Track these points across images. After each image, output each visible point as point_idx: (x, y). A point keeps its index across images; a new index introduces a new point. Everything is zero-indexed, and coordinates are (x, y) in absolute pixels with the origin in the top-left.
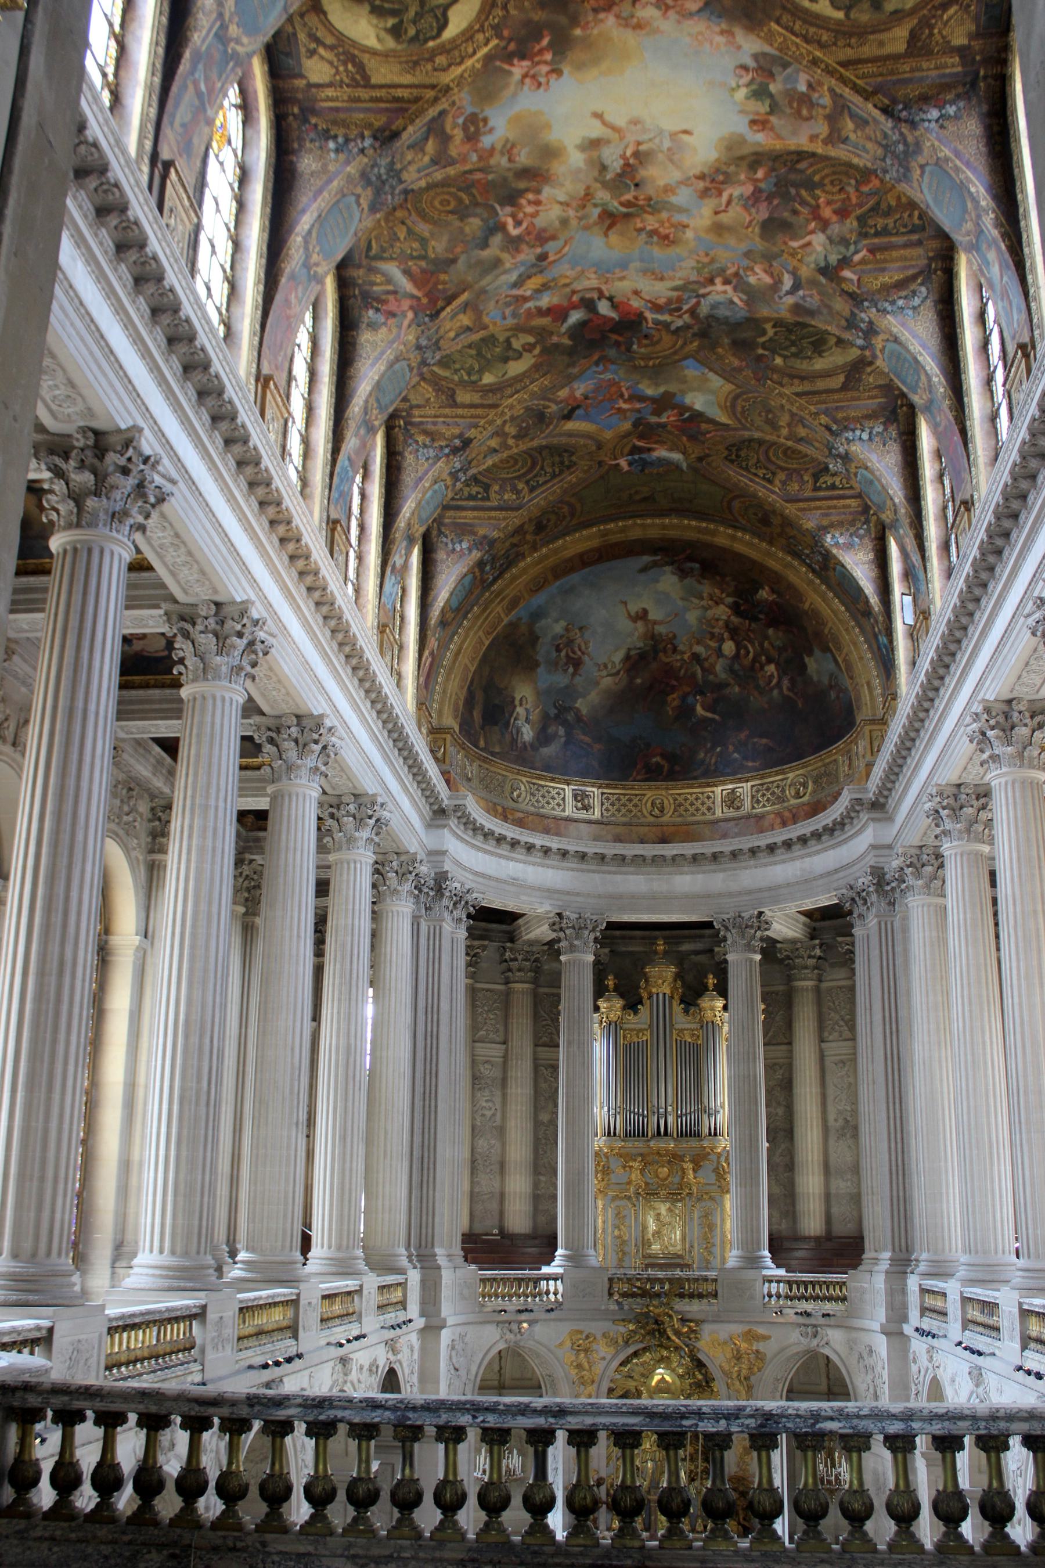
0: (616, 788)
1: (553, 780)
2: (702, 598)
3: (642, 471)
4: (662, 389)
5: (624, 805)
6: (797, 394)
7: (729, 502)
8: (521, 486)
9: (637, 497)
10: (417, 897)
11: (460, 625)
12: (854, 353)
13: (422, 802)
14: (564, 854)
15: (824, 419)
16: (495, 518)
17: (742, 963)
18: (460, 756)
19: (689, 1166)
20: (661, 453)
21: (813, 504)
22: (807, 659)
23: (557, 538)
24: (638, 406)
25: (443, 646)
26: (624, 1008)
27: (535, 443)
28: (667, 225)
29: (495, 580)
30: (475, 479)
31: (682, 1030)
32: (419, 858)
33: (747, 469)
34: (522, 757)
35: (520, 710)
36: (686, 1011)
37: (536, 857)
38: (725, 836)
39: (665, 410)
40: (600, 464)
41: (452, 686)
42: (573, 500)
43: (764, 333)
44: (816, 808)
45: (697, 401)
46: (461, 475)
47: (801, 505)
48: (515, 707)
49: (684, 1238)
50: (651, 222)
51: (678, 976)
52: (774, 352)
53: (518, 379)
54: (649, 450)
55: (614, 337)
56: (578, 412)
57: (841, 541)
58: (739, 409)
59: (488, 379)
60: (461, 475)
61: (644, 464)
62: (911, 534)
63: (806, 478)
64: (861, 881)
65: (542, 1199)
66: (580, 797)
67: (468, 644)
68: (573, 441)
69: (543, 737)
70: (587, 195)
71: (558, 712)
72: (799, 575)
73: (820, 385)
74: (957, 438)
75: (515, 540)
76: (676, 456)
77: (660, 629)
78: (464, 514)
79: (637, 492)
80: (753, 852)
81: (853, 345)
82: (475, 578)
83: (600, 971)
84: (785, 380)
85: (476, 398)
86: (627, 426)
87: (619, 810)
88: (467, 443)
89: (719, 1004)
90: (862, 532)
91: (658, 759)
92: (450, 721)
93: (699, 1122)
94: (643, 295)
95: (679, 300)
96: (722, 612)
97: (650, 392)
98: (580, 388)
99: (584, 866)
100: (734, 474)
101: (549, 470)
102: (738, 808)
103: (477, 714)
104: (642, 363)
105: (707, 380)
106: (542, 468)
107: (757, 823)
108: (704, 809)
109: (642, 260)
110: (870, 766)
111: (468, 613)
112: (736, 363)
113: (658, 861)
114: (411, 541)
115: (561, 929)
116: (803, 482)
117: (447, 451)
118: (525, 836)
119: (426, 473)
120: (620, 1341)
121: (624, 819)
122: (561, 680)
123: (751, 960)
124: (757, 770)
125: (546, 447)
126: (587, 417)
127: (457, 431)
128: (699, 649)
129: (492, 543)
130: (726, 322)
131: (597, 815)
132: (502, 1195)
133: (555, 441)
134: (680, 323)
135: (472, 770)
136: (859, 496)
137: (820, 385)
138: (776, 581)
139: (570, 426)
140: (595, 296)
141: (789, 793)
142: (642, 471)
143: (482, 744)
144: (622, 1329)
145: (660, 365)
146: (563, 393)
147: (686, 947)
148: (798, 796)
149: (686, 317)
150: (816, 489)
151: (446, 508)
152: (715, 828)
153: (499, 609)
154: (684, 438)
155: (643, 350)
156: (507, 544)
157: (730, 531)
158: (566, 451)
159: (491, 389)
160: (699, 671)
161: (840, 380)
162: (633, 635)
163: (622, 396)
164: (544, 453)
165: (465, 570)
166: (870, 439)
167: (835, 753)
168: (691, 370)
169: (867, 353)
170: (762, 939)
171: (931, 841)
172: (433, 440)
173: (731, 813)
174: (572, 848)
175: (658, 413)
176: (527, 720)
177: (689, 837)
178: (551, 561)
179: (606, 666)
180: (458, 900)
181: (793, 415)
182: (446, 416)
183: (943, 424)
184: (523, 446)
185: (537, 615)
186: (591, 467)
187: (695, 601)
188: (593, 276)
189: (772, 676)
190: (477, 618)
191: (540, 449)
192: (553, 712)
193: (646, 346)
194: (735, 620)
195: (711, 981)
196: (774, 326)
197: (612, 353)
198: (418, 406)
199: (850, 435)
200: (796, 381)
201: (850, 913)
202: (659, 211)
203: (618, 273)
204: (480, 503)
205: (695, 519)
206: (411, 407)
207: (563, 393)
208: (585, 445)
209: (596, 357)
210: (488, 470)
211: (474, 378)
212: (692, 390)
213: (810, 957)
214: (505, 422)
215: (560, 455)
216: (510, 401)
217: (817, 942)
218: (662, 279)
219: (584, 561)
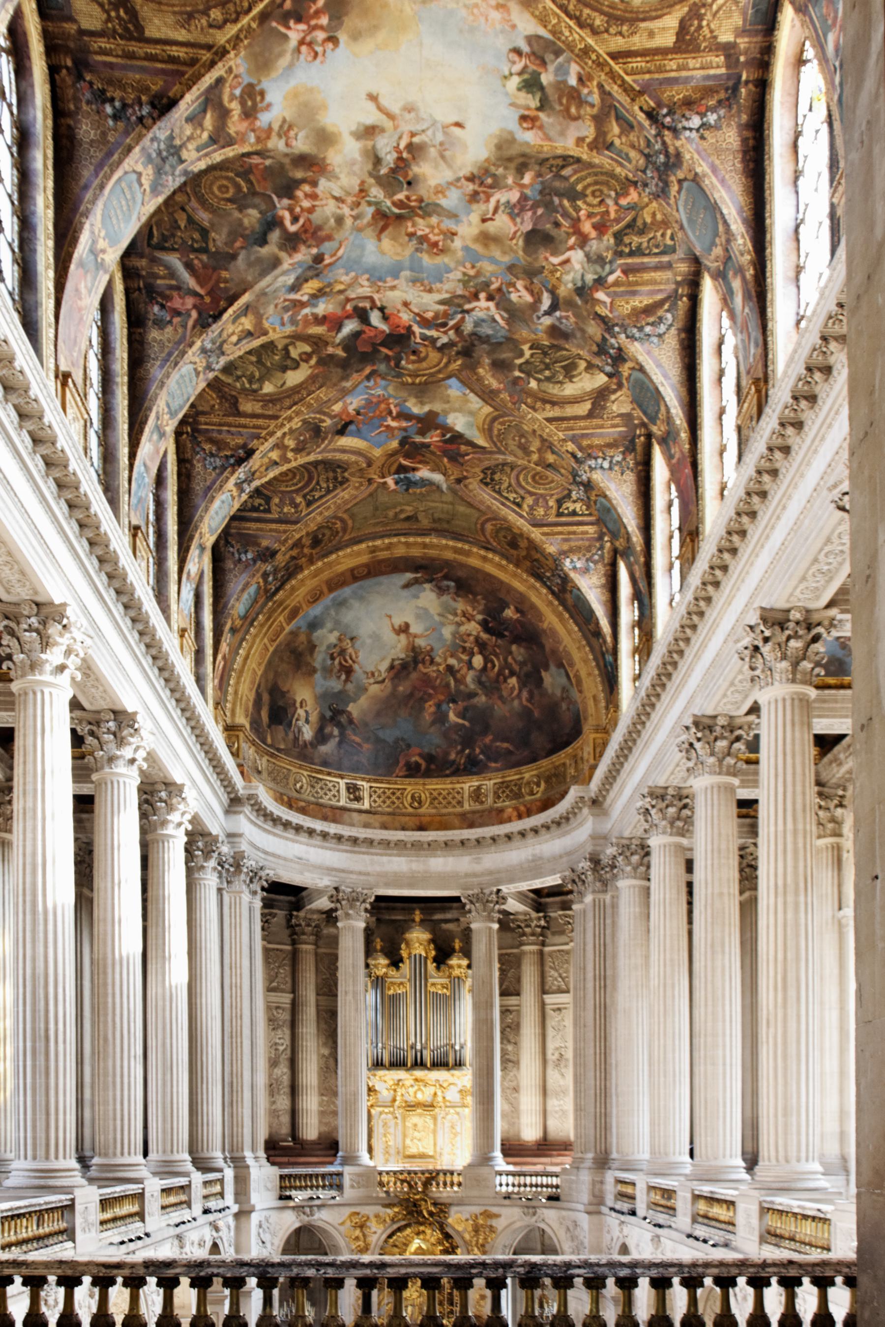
2: (456, 615)
3: (407, 490)
4: (426, 408)
7: (483, 524)
8: (299, 500)
16: (275, 531)
20: (424, 473)
23: (331, 553)
24: (404, 424)
28: (436, 231)
30: (257, 492)
33: (499, 492)
39: (429, 430)
40: (370, 481)
42: (345, 516)
45: (458, 422)
46: (245, 486)
50: (421, 226)
54: (414, 469)
56: (352, 428)
59: (268, 388)
61: (409, 484)
70: (361, 191)
76: (438, 477)
78: (248, 525)
79: (402, 511)
86: (395, 444)
94: (412, 307)
95: (446, 315)
97: (416, 410)
105: (467, 401)
106: (318, 483)
109: (412, 269)
113: (417, 846)
125: (324, 462)
130: (485, 340)
133: (329, 456)
134: (444, 340)
139: (345, 441)
140: (368, 305)
142: (407, 490)
145: (426, 383)
149: (451, 333)
155: (410, 366)
157: (482, 552)
158: (339, 467)
159: (271, 400)
164: (320, 468)
175: (422, 432)
178: (326, 575)
184: (302, 460)
186: (361, 484)
188: (366, 283)
193: (414, 362)
197: (382, 367)
202: (430, 215)
203: (390, 282)
205: (453, 539)
208: (356, 463)
212: (455, 410)
215: (334, 471)
218: (430, 291)
219: (355, 576)
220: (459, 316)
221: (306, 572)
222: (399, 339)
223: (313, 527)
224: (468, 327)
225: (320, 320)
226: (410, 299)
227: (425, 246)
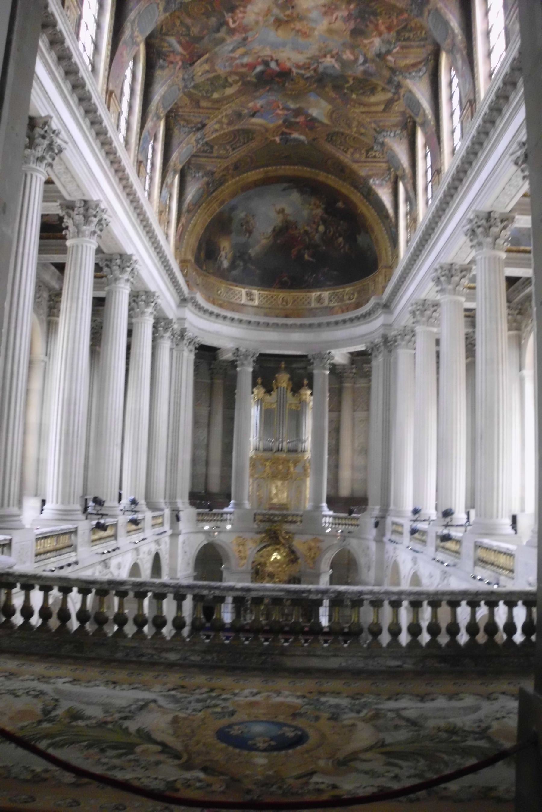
0: (266, 291)
1: (237, 286)
2: (310, 204)
4: (298, 106)
5: (269, 299)
6: (363, 113)
8: (228, 147)
9: (283, 155)
10: (172, 339)
11: (196, 212)
12: (389, 95)
13: (176, 295)
14: (241, 321)
15: (373, 125)
17: (321, 375)
18: (194, 273)
19: (291, 465)
20: (295, 135)
21: (365, 164)
22: (357, 236)
23: (244, 173)
25: (188, 222)
26: (265, 393)
27: (236, 127)
29: (214, 191)
30: (207, 143)
31: (290, 404)
32: (174, 321)
33: (335, 146)
34: (223, 275)
35: (223, 253)
36: (294, 395)
37: (228, 322)
38: (315, 316)
40: (266, 139)
41: (192, 241)
43: (348, 82)
44: (358, 305)
45: (314, 112)
46: (200, 141)
47: (360, 164)
48: (220, 252)
49: (288, 497)
51: (291, 379)
52: (352, 91)
53: (230, 97)
54: (290, 134)
55: (277, 79)
56: (258, 114)
57: (377, 182)
58: (334, 116)
60: (200, 141)
62: (411, 181)
63: (363, 152)
64: (376, 340)
65: (226, 477)
66: (249, 295)
67: (200, 222)
68: (255, 127)
69: (233, 265)
71: (240, 255)
72: (356, 197)
73: (373, 109)
74: (435, 139)
75: (224, 173)
76: (302, 137)
77: (290, 218)
80: (328, 324)
81: (389, 91)
82: (204, 190)
83: (255, 375)
84: (356, 105)
85: (209, 105)
86: (281, 122)
87: (267, 301)
88: (204, 126)
89: (309, 392)
90: (387, 179)
91: (285, 279)
92: (190, 257)
93: (297, 445)
96: (319, 212)
97: (292, 106)
98: (259, 103)
99: (250, 327)
100: (329, 148)
101: (242, 140)
102: (322, 303)
103: (202, 254)
104: (290, 93)
106: (239, 140)
107: (330, 310)
108: (306, 303)
110: (384, 288)
111: (199, 207)
112: (334, 95)
114: (175, 172)
115: (238, 356)
116: (361, 154)
117: (194, 129)
118: (223, 312)
119: (184, 139)
120: (258, 542)
121: (270, 306)
122: (242, 239)
123: (324, 374)
124: (330, 286)
126: (262, 116)
127: (199, 120)
128: (307, 228)
129: (213, 173)
131: (256, 303)
132: (207, 476)
133: (246, 127)
134: (308, 75)
135: (199, 280)
136: (387, 162)
137: (373, 109)
138: (346, 200)
139: (254, 120)
141: (346, 297)
143: (204, 268)
144: (259, 536)
146: (251, 105)
147: (294, 366)
148: (349, 299)
149: (312, 72)
150: (368, 157)
151: (193, 156)
152: (312, 313)
153: (215, 205)
154: (307, 130)
156: (221, 174)
157: (325, 174)
160: (307, 240)
161: (382, 107)
162: (277, 220)
163: (279, 107)
165: (200, 186)
166: (394, 136)
167: (368, 281)
168: (312, 98)
169: (396, 97)
170: (330, 364)
171: (410, 324)
172: (188, 124)
173: (318, 305)
174: (245, 318)
175: (296, 116)
176: (226, 257)
177: (299, 316)
179: (264, 234)
180: (191, 341)
181: (359, 122)
182: (194, 112)
183: (429, 133)
184: (231, 128)
185: (233, 209)
187: (307, 206)
189: (341, 243)
190: (205, 209)
191: (238, 131)
192: (238, 254)
194: (325, 216)
195: (306, 382)
196: (354, 79)
197: (276, 87)
198: (181, 107)
199: (385, 134)
200: (362, 107)
201: (371, 354)
204: (208, 155)
206: (178, 107)
207: (251, 105)
209: (268, 88)
210: (213, 139)
211: (209, 95)
213: (351, 373)
214: (222, 117)
216: (225, 107)
217: (354, 366)
220: (316, 65)
221: (230, 182)
222: (284, 75)
223: (235, 160)
224: (321, 69)
225: (243, 65)
226: (292, 55)
227: (300, 33)
